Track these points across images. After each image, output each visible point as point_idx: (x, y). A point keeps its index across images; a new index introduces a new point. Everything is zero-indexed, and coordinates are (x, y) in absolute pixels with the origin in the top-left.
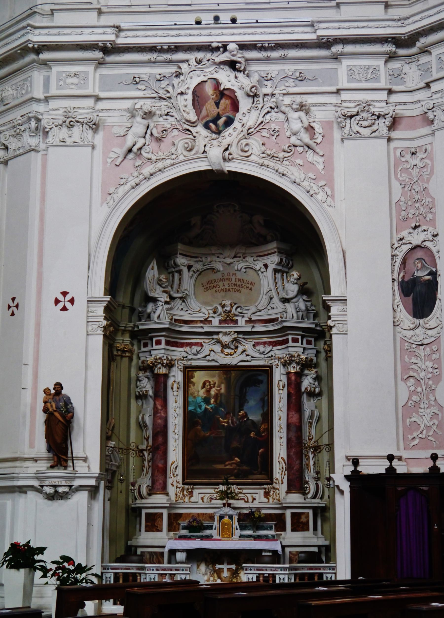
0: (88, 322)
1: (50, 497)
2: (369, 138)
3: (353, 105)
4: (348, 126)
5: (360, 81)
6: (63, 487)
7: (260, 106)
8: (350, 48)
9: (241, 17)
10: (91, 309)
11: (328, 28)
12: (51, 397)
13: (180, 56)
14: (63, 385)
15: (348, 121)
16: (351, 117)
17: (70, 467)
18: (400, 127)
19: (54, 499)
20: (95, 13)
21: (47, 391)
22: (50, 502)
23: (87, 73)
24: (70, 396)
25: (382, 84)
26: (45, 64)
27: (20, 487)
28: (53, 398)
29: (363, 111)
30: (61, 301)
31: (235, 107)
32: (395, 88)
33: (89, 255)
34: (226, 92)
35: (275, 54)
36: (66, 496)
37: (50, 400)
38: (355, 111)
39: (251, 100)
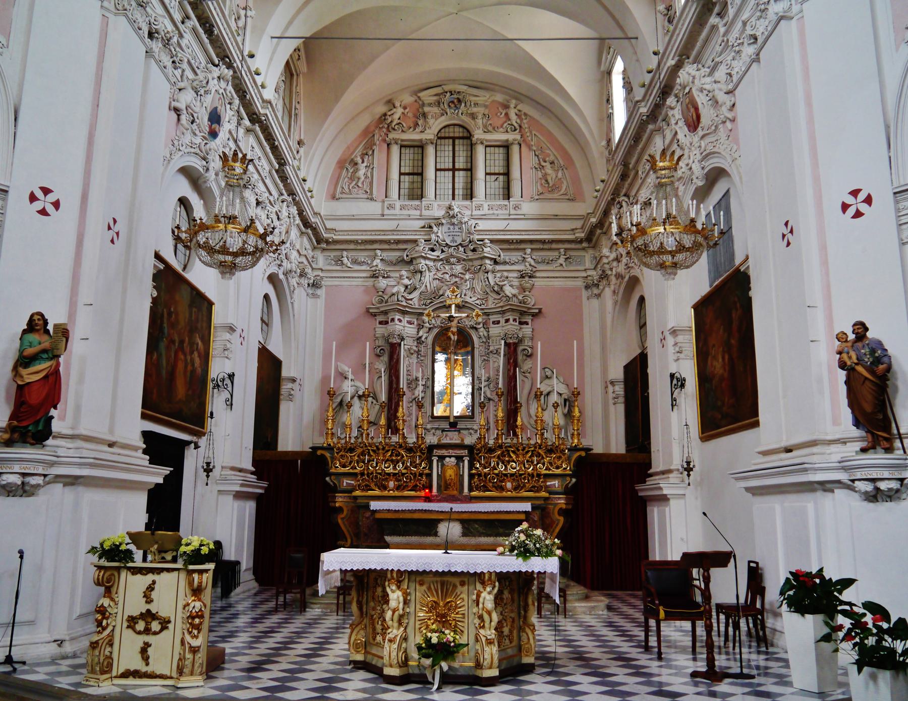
0: (901, 225)
1: (875, 496)
6: (887, 482)
10: (901, 206)
12: (850, 344)
14: (868, 325)
17: (898, 449)
19: (878, 501)
21: (841, 337)
22: (871, 505)
24: (881, 339)
27: (822, 483)
28: (852, 346)
30: (851, 205)
33: (887, 127)
36: (897, 495)
37: (846, 349)
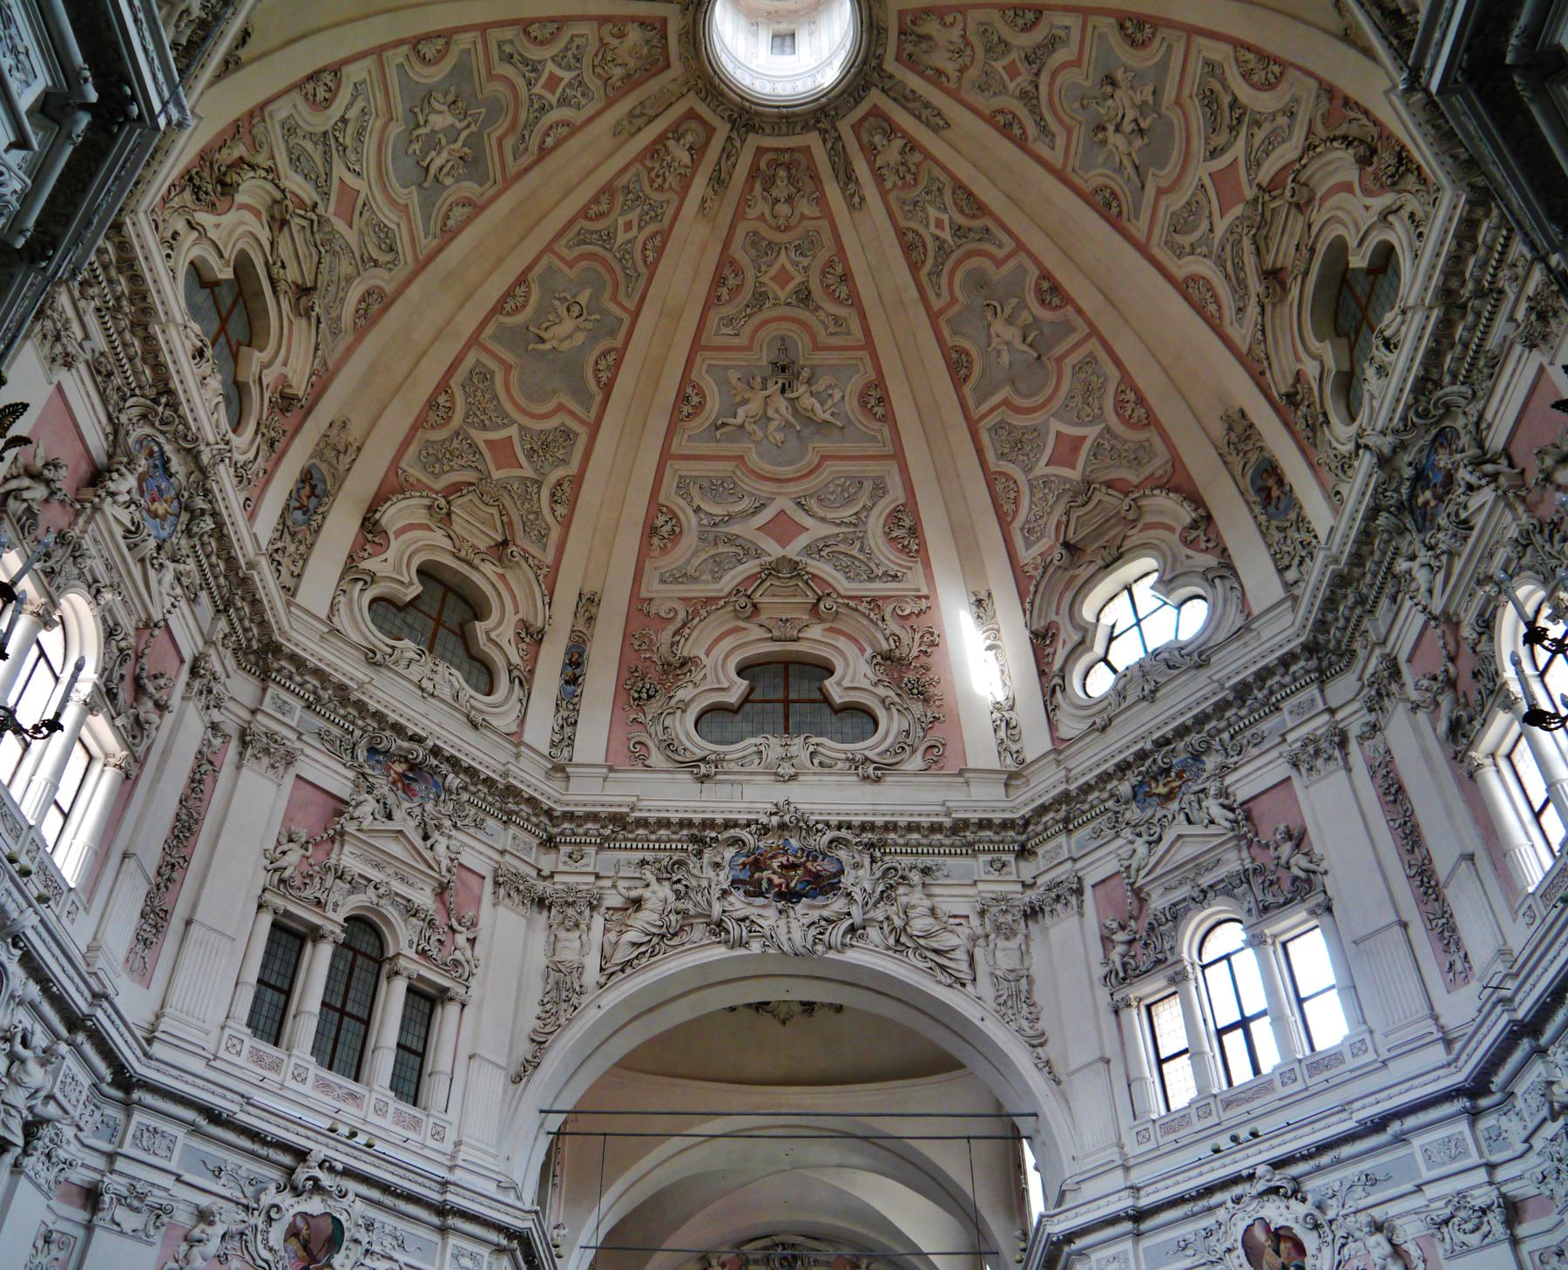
2: (1481, 1248)
3: (1441, 1204)
4: (1447, 1237)
5: (1444, 1163)
7: (1329, 1239)
8: (1411, 1122)
9: (1263, 1127)
11: (1364, 1107)
13: (1218, 1198)
15: (1444, 1229)
16: (1446, 1222)
18: (1527, 1216)
20: (1120, 1172)
23: (1125, 1252)
25: (1475, 1159)
26: (1081, 1253)
29: (1457, 1209)
31: (1300, 1249)
32: (1495, 1158)
34: (1282, 1232)
35: (1325, 1159)
38: (1447, 1212)
39: (1315, 1234)
